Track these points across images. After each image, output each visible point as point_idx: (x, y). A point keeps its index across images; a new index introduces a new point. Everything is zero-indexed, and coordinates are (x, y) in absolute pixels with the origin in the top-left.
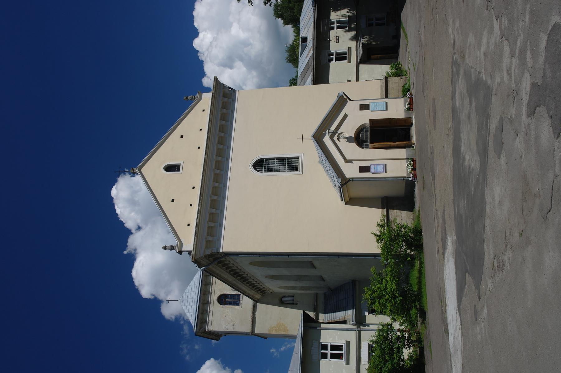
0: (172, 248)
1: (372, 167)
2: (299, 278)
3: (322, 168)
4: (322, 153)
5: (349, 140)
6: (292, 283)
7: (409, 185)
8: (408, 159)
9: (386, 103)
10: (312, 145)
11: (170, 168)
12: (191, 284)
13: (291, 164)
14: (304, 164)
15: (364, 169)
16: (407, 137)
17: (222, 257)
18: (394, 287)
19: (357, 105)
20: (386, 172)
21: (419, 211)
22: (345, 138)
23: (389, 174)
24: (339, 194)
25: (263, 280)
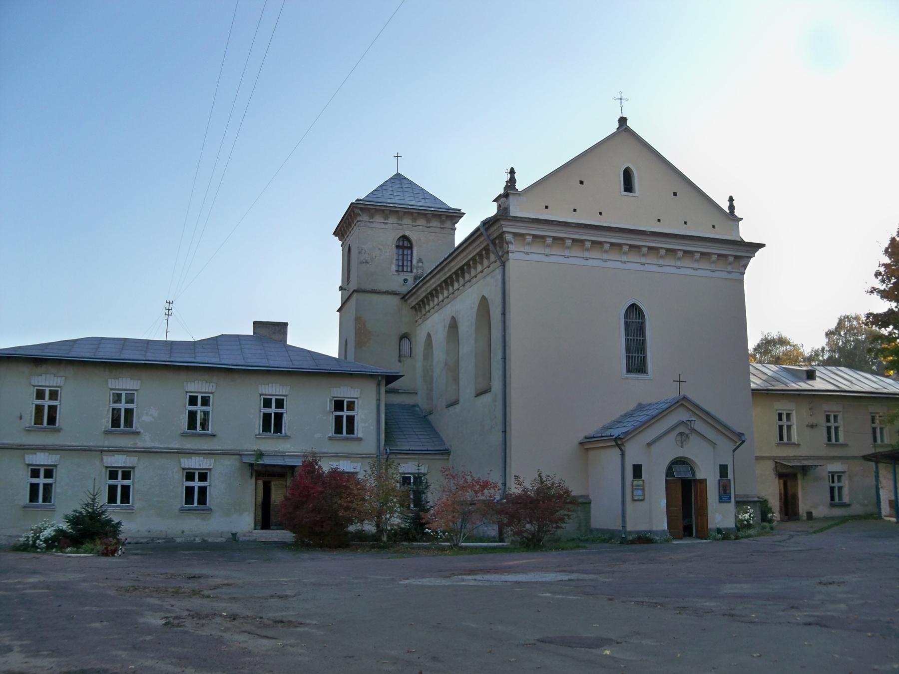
0: (512, 182)
1: (640, 482)
6: (439, 354)
10: (672, 394)
11: (628, 176)
13: (637, 362)
15: (637, 471)
17: (500, 258)
19: (728, 462)
20: (634, 500)
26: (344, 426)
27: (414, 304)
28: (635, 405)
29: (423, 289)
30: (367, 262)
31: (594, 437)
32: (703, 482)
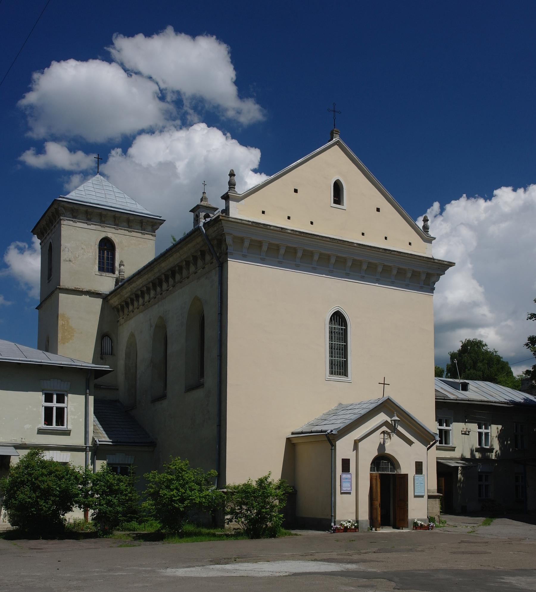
2: (161, 366)
3: (333, 408)
4: (368, 410)
5: (382, 447)
7: (324, 523)
8: (357, 521)
9: (422, 496)
10: (376, 396)
12: (126, 196)
13: (339, 366)
14: (338, 384)
16: (385, 523)
18: (198, 500)
20: (342, 493)
21: (296, 535)
22: (384, 442)
23: (340, 499)
24: (300, 430)
25: (155, 312)
26: (54, 417)
27: (117, 303)
28: (336, 405)
29: (129, 289)
30: (70, 261)
31: (302, 433)
32: (405, 477)
